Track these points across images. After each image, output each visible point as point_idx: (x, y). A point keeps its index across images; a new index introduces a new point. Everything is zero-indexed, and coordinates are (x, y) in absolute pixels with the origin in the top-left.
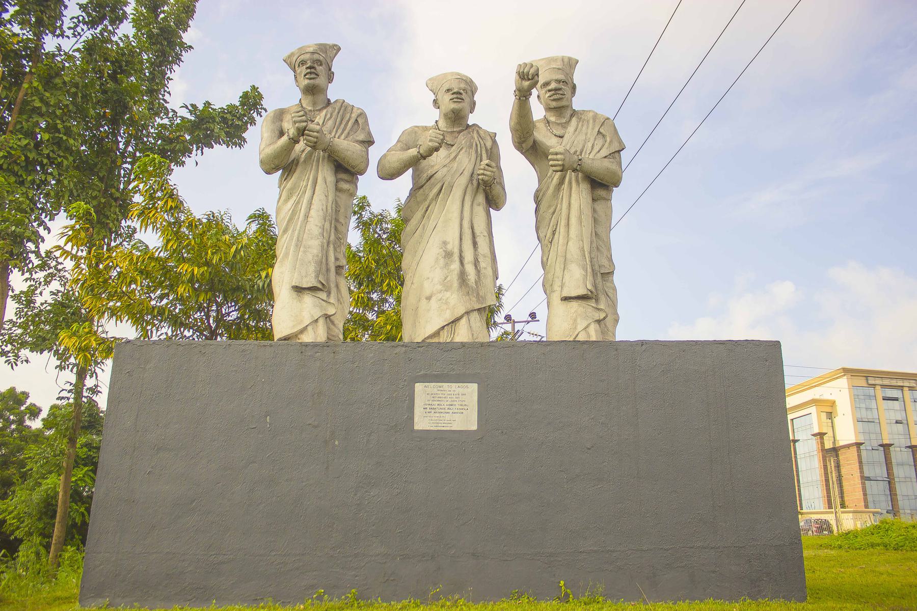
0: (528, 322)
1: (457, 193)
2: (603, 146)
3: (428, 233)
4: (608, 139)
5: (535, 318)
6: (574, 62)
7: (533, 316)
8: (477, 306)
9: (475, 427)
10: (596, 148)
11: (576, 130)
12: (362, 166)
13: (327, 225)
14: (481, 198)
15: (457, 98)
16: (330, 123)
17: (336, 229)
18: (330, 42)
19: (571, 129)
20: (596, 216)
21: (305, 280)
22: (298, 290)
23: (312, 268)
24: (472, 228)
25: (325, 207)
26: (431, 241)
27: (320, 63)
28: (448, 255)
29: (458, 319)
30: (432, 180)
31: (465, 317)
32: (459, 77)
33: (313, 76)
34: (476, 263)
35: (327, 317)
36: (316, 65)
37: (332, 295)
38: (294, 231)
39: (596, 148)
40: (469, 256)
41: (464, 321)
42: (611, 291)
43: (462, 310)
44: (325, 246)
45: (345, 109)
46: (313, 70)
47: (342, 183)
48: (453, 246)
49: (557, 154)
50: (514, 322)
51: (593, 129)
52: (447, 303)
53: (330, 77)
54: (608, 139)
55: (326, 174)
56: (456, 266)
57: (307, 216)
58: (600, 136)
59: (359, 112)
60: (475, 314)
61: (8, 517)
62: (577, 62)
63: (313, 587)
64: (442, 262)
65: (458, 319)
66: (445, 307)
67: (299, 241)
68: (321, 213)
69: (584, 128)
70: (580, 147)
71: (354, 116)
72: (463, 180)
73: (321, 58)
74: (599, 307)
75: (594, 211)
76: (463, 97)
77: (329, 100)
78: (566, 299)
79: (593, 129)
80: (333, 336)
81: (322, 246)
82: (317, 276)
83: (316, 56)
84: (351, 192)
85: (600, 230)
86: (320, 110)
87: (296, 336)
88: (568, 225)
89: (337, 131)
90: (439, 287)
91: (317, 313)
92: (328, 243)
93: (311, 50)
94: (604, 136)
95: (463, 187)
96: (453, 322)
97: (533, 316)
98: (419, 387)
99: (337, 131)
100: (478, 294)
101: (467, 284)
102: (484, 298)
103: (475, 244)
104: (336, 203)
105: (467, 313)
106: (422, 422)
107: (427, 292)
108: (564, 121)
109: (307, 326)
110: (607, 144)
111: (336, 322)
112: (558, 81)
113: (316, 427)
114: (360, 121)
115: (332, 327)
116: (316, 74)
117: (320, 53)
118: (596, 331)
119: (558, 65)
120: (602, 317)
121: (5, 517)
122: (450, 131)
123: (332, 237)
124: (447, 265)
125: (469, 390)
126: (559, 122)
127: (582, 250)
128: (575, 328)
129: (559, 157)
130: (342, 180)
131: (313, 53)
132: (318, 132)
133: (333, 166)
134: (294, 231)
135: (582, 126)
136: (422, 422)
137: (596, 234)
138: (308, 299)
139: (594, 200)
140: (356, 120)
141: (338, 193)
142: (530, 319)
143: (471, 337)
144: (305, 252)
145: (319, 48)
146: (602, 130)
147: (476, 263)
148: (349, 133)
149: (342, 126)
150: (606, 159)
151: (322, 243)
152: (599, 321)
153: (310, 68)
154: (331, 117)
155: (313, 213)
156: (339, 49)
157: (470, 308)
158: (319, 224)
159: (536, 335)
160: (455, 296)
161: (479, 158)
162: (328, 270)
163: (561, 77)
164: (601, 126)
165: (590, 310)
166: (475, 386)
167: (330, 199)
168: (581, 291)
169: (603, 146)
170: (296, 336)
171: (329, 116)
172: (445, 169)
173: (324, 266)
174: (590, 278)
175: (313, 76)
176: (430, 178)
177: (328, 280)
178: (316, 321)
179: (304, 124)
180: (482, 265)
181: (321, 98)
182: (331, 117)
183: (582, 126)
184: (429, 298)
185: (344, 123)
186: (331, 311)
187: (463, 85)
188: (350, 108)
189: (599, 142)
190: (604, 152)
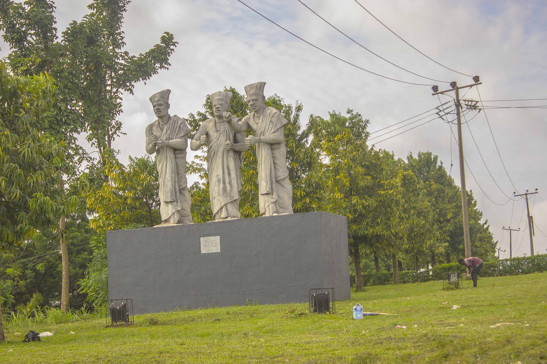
0: (471, 86)
1: (220, 154)
2: (272, 127)
3: (213, 170)
4: (274, 124)
5: (478, 81)
6: (263, 85)
7: (476, 79)
8: (229, 201)
9: (220, 251)
10: (269, 130)
11: (262, 121)
12: (184, 148)
13: (173, 175)
14: (231, 154)
15: (217, 111)
16: (169, 132)
17: (178, 173)
18: (165, 88)
19: (260, 121)
20: (275, 156)
21: (167, 199)
22: (166, 203)
23: (169, 195)
24: (228, 168)
25: (171, 168)
26: (213, 176)
27: (161, 105)
28: (219, 180)
29: (222, 208)
30: (211, 149)
31: (224, 208)
32: (219, 98)
33: (159, 113)
34: (230, 183)
35: (178, 211)
36: (160, 107)
37: (178, 203)
38: (162, 178)
39: (269, 130)
40: (227, 180)
41: (224, 209)
42: (287, 185)
43: (223, 204)
44: (174, 184)
45: (175, 122)
46: (158, 110)
47: (178, 155)
48: (221, 177)
49: (247, 140)
50: (458, 88)
51: (268, 120)
52: (219, 201)
53: (168, 106)
54: (274, 124)
55: (170, 154)
56: (221, 185)
57: (166, 172)
58: (271, 123)
59: (181, 122)
60: (230, 204)
61: (88, 291)
62: (265, 83)
63: (175, 306)
64: (217, 184)
65: (222, 208)
66: (219, 202)
67: (164, 183)
68: (170, 171)
69: (265, 120)
70: (263, 129)
71: (179, 125)
72: (221, 149)
73: (162, 102)
74: (274, 197)
75: (272, 153)
76: (220, 109)
77: (169, 115)
78: (262, 194)
79: (268, 120)
80: (186, 215)
81: (172, 185)
82: (171, 197)
83: (159, 102)
84: (182, 157)
85: (276, 162)
86: (165, 124)
87: (168, 219)
88: (261, 163)
89: (172, 135)
90: (217, 194)
91: (174, 211)
92: (175, 182)
93: (157, 99)
94: (273, 123)
95: (222, 152)
96: (221, 208)
97: (476, 79)
98: (202, 239)
99: (172, 135)
100: (231, 195)
101: (227, 192)
102: (233, 197)
103: (229, 174)
104: (176, 163)
105: (226, 205)
106: (203, 251)
107: (214, 196)
108: (260, 115)
109: (171, 216)
110: (274, 127)
111: (186, 209)
112: (254, 100)
113: (171, 255)
114: (182, 126)
115: (183, 211)
116: (160, 111)
117: (161, 100)
118: (272, 207)
119: (253, 91)
120: (275, 201)
121: (87, 291)
122: (219, 122)
123: (177, 179)
124: (219, 185)
125: (217, 238)
126: (258, 116)
127: (266, 174)
128: (265, 206)
129: (248, 141)
130: (178, 154)
131: (158, 101)
132: (161, 144)
133: (172, 150)
134: (162, 178)
135: (265, 119)
136: (203, 251)
137: (274, 163)
138: (170, 206)
139: (272, 149)
140: (180, 127)
141: (177, 159)
142: (474, 83)
143: (226, 214)
144: (166, 188)
145: (160, 97)
146: (272, 120)
147: (230, 183)
148: (177, 134)
149: (174, 132)
150: (272, 134)
151: (172, 183)
152: (275, 203)
153: (157, 109)
154: (169, 129)
155: (167, 171)
156: (170, 91)
157: (226, 202)
158: (170, 176)
159: (470, 101)
160: (221, 198)
161: (228, 137)
162: (176, 193)
163: (254, 98)
164: (272, 118)
165: (270, 198)
166: (219, 237)
167: (174, 163)
168: (265, 192)
169: (272, 127)
170: (168, 219)
171: (168, 129)
172: (215, 144)
173: (174, 193)
174: (269, 186)
175: (159, 113)
176: (211, 147)
177: (176, 197)
178: (174, 213)
179: (155, 141)
180: (233, 182)
181: (166, 119)
182: (169, 129)
183: (265, 119)
184: (214, 199)
185: (174, 130)
186: (179, 209)
187: (220, 103)
188: (177, 121)
189: (271, 126)
190: (272, 131)
